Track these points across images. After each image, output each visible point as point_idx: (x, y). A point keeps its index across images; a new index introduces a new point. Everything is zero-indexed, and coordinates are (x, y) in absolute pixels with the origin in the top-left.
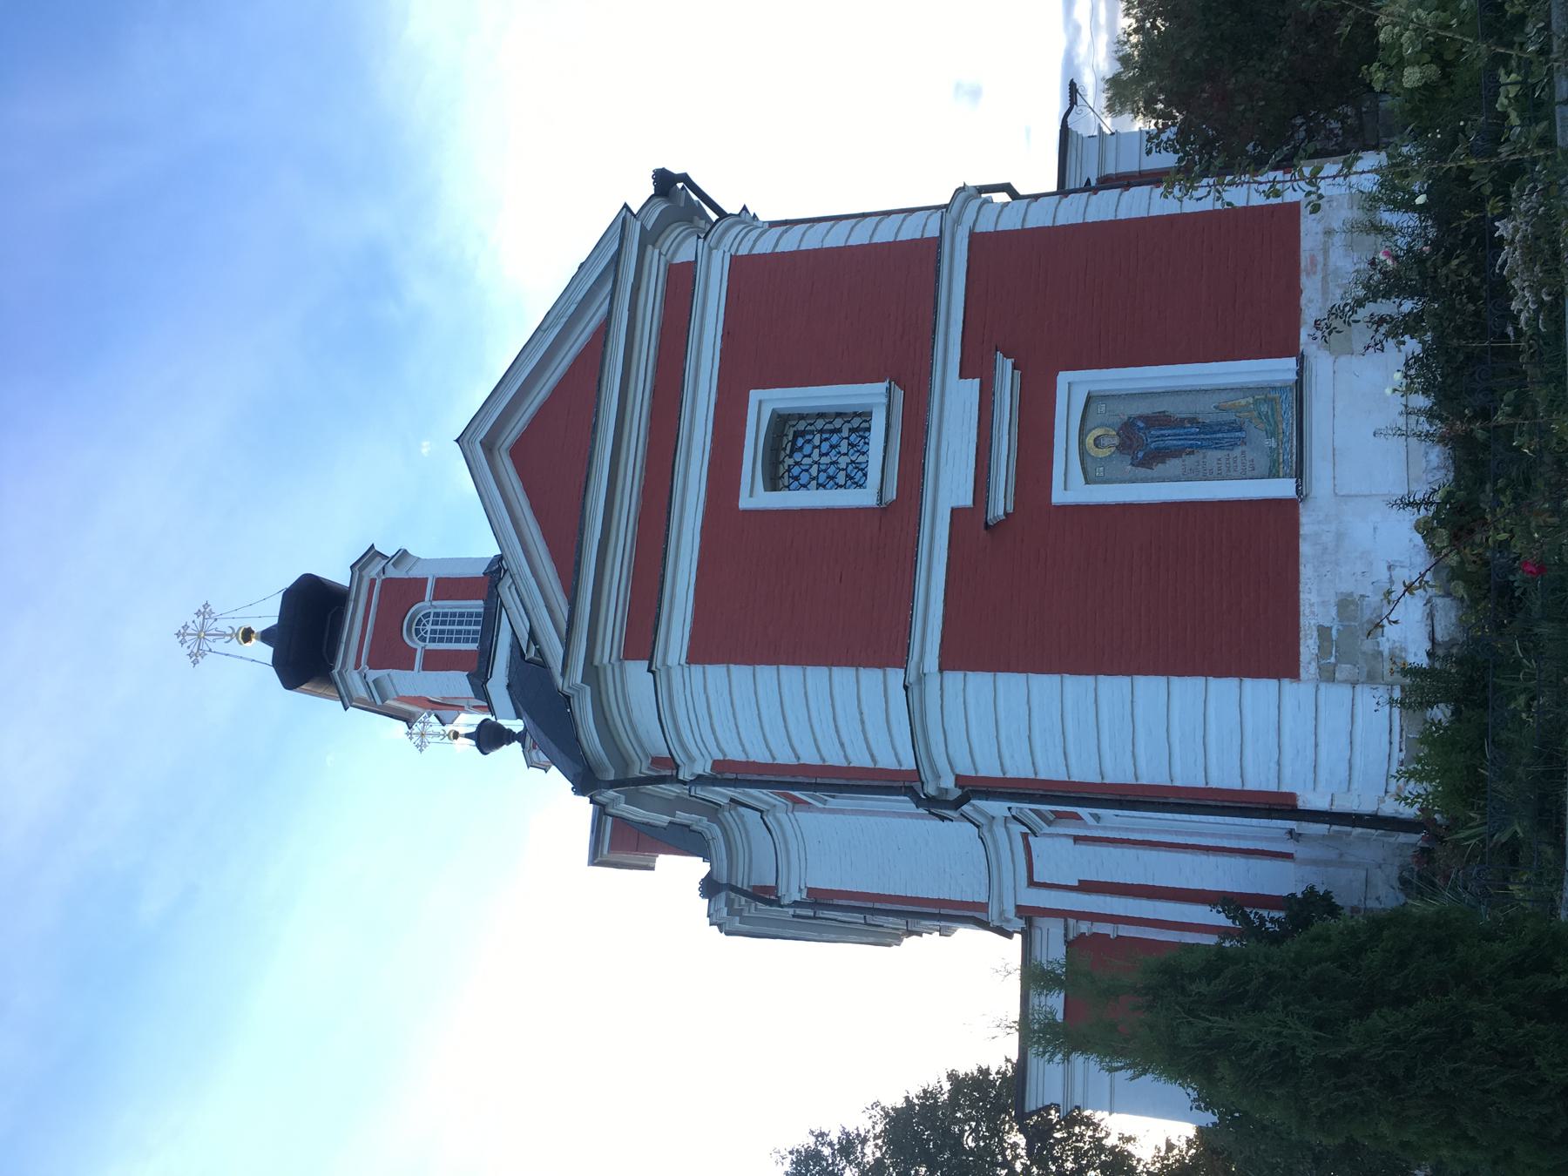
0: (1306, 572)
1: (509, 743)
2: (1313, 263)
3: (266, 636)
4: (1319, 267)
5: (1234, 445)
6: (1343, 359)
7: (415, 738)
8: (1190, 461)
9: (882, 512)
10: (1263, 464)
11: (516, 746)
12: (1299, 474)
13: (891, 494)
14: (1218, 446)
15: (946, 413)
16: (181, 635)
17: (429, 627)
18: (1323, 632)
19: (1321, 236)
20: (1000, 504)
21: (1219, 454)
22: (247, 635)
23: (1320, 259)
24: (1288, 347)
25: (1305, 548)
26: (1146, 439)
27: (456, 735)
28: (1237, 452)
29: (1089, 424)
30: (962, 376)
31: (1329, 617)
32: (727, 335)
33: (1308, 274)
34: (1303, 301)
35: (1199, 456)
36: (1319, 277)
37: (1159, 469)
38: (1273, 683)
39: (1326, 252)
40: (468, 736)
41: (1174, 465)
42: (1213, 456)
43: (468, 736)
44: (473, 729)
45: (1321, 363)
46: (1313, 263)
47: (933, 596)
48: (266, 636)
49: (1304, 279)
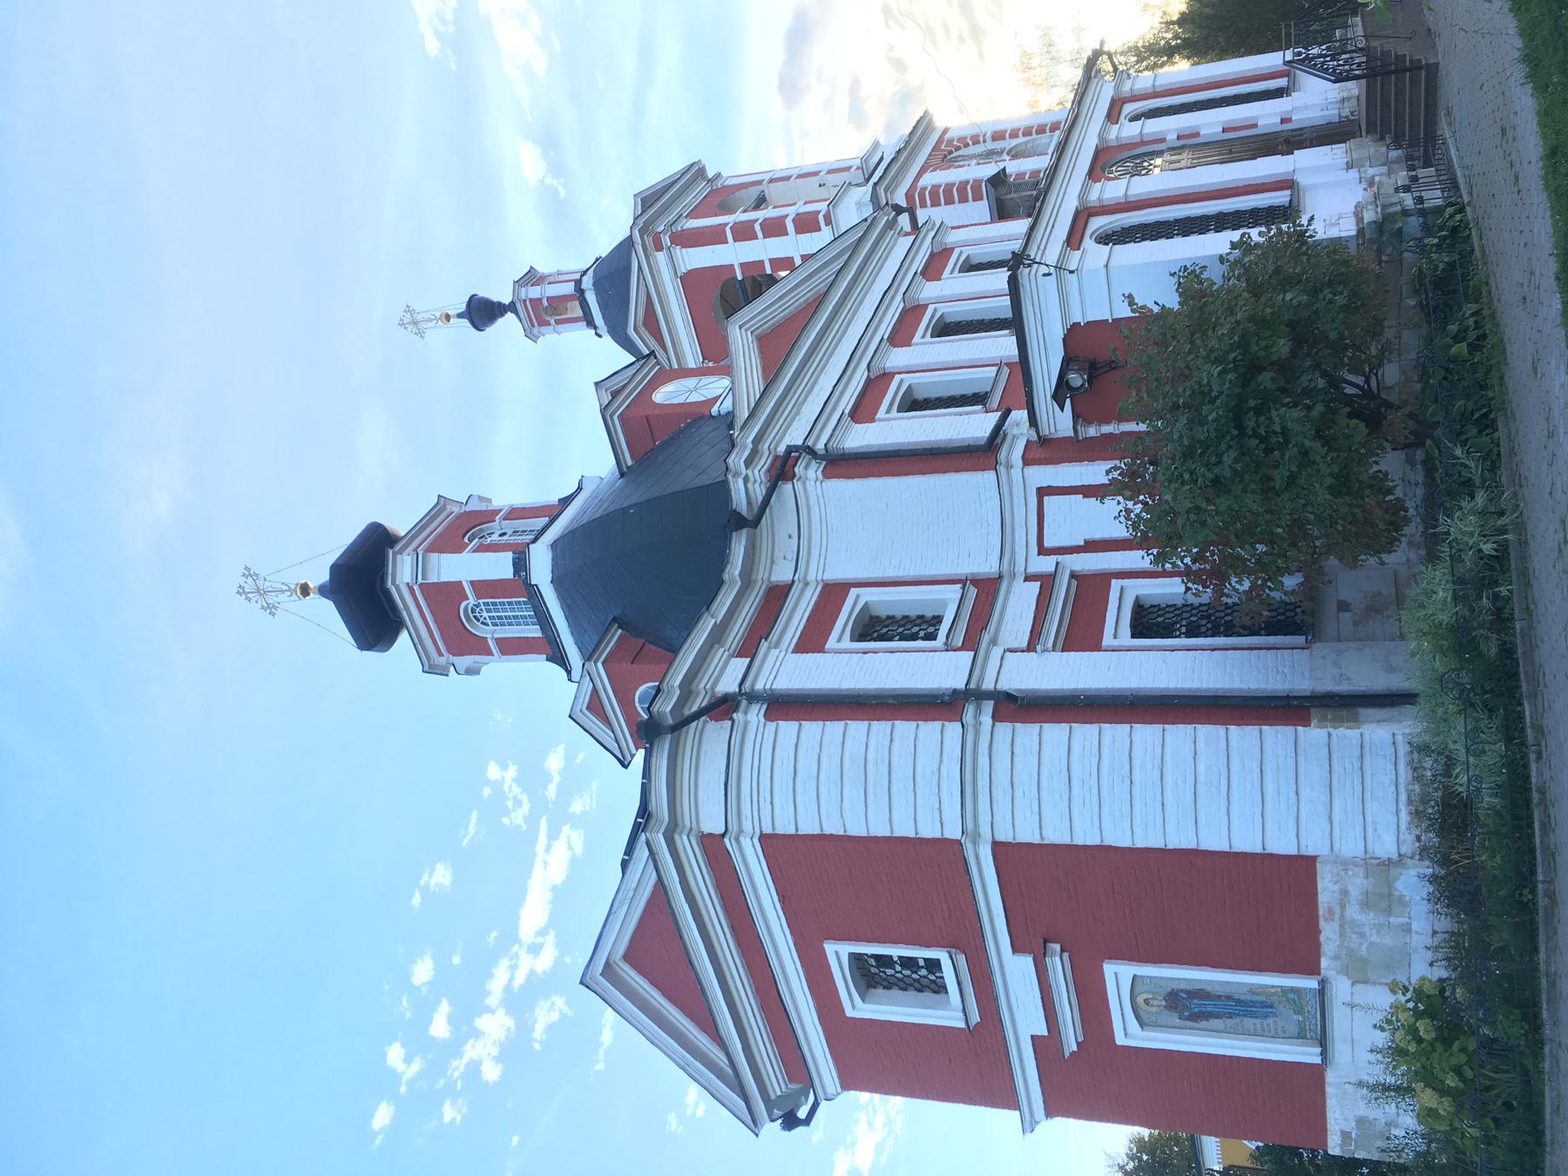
0: (1332, 1104)
1: (502, 315)
2: (1330, 910)
3: (323, 591)
4: (1337, 917)
5: (1266, 1016)
6: (1359, 986)
7: (410, 327)
8: (1229, 1022)
9: (970, 1030)
10: (1294, 1030)
11: (510, 316)
12: (1323, 1042)
13: (975, 1018)
14: (1254, 1015)
15: (1009, 980)
16: (241, 591)
17: (485, 614)
18: (1345, 1135)
19: (1337, 895)
20: (1071, 1044)
21: (1257, 1021)
22: (305, 590)
23: (1338, 910)
24: (1312, 969)
25: (1328, 1089)
26: (1188, 1006)
27: (448, 317)
28: (1270, 1021)
29: (1137, 990)
30: (1016, 948)
31: (1350, 1126)
32: (783, 899)
33: (1326, 920)
34: (1322, 938)
35: (1238, 1020)
36: (1336, 924)
37: (1203, 1024)
38: (1289, 730)
39: (1343, 907)
40: (460, 316)
41: (1216, 1023)
42: (1249, 1022)
43: (460, 316)
44: (463, 308)
45: (1341, 988)
46: (1330, 910)
47: (1030, 1081)
48: (323, 591)
49: (1322, 923)
